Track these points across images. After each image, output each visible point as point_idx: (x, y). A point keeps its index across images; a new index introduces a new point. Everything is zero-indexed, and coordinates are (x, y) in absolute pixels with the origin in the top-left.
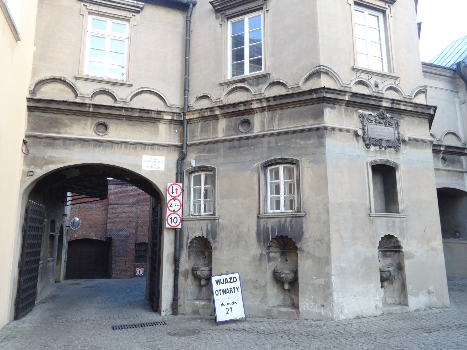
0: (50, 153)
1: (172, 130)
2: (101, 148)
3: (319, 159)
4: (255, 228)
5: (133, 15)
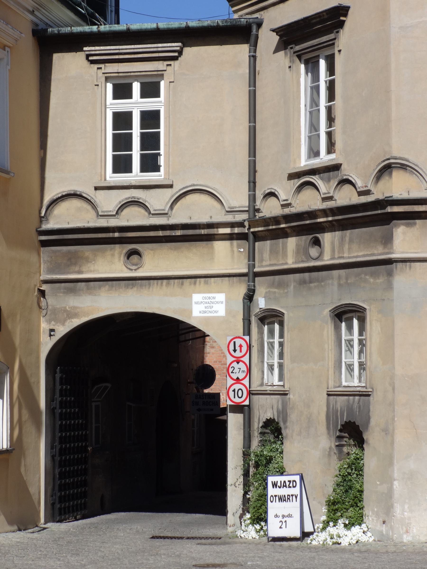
0: (73, 302)
1: (235, 249)
2: (135, 289)
4: (325, 409)
5: (168, 65)
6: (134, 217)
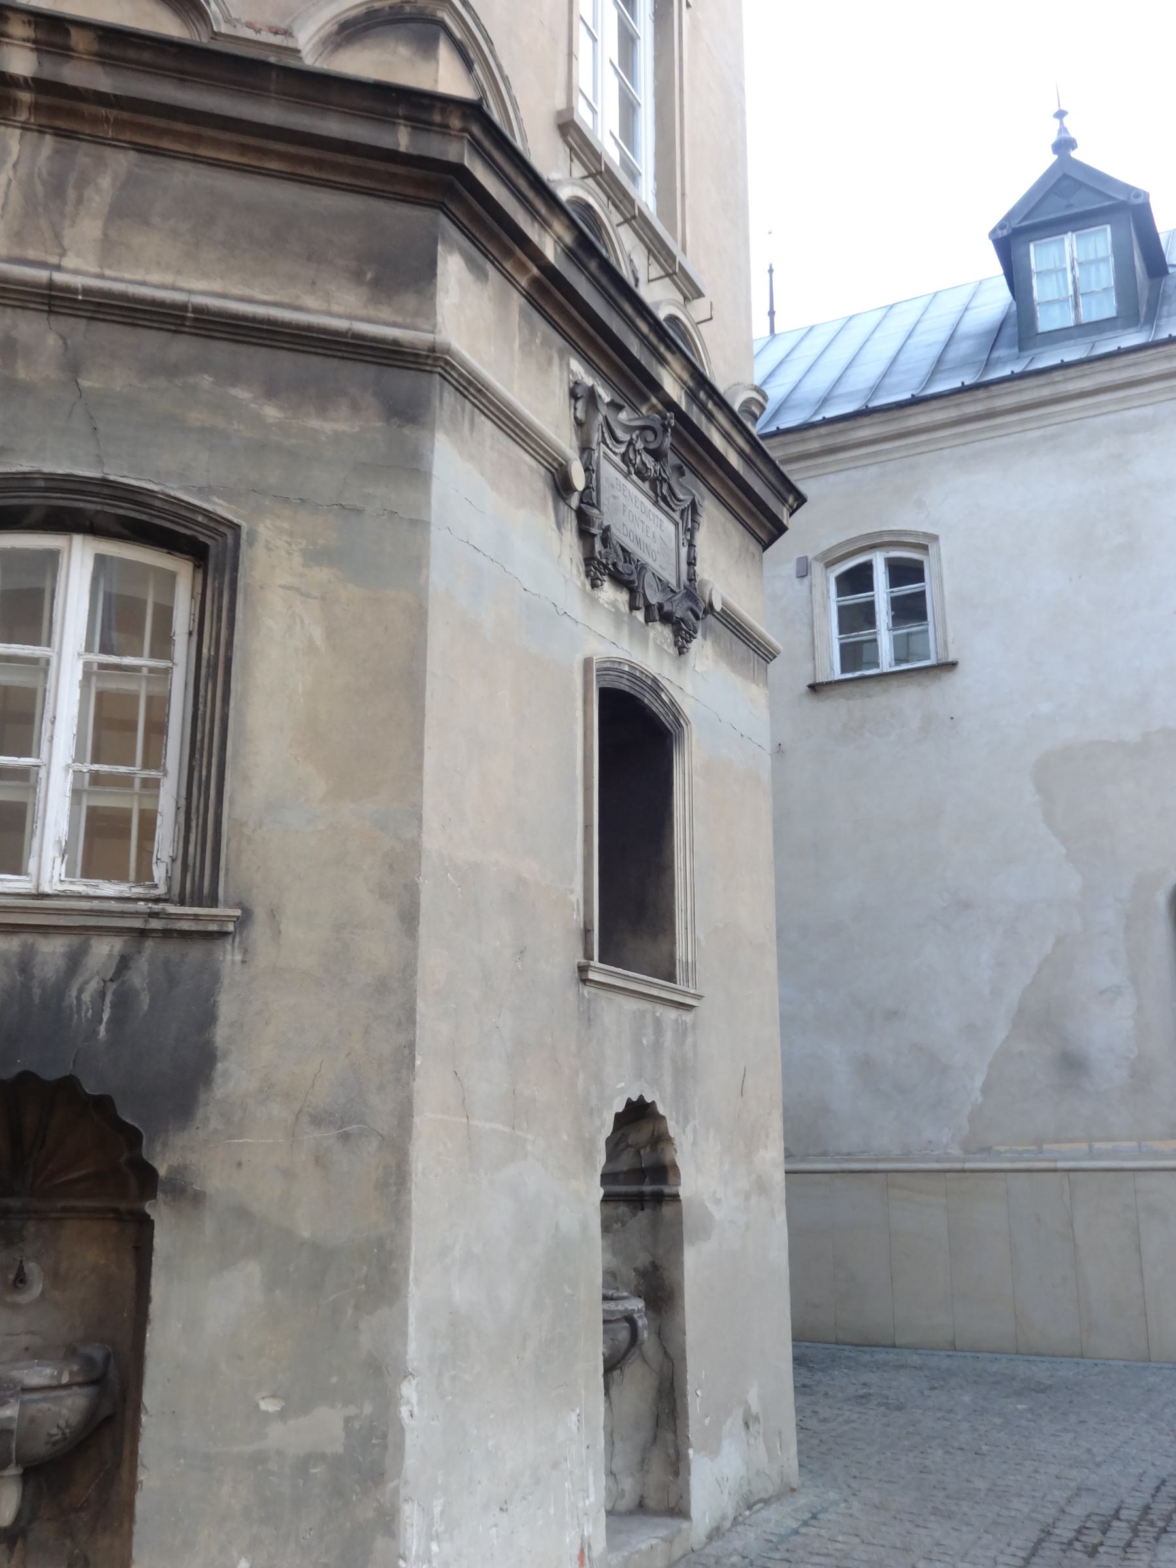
3: (383, 549)
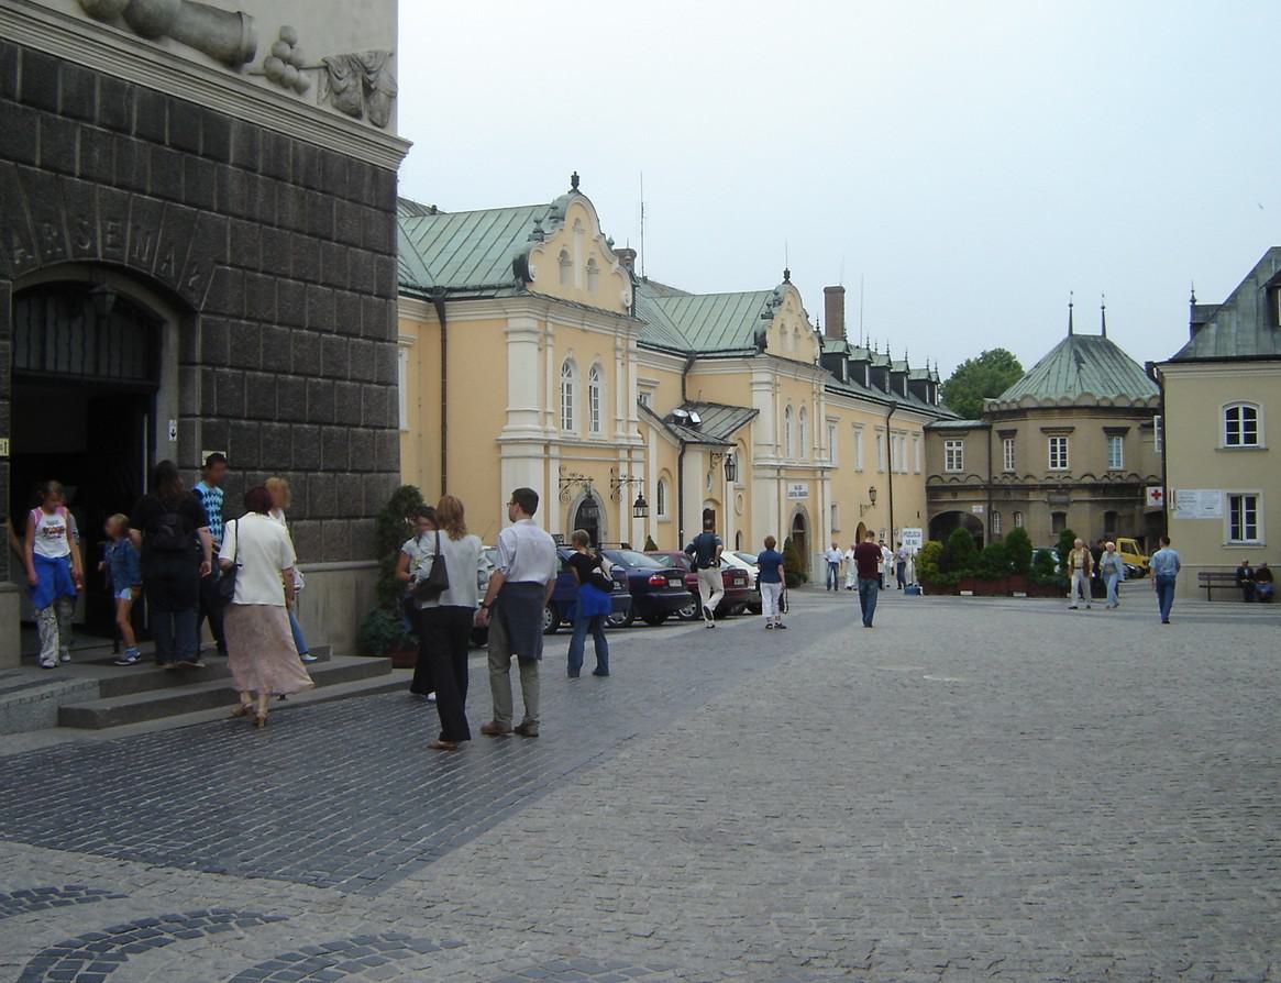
0: (936, 508)
6: (955, 483)
